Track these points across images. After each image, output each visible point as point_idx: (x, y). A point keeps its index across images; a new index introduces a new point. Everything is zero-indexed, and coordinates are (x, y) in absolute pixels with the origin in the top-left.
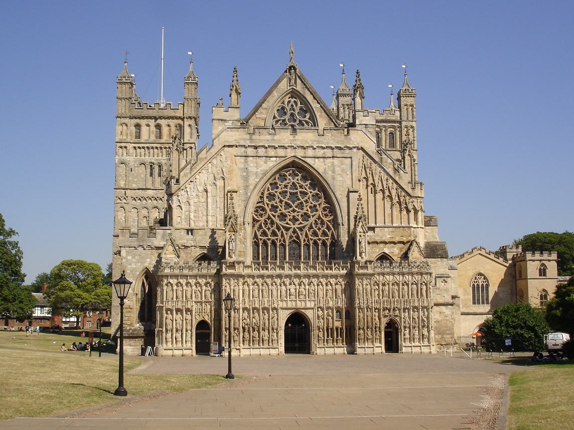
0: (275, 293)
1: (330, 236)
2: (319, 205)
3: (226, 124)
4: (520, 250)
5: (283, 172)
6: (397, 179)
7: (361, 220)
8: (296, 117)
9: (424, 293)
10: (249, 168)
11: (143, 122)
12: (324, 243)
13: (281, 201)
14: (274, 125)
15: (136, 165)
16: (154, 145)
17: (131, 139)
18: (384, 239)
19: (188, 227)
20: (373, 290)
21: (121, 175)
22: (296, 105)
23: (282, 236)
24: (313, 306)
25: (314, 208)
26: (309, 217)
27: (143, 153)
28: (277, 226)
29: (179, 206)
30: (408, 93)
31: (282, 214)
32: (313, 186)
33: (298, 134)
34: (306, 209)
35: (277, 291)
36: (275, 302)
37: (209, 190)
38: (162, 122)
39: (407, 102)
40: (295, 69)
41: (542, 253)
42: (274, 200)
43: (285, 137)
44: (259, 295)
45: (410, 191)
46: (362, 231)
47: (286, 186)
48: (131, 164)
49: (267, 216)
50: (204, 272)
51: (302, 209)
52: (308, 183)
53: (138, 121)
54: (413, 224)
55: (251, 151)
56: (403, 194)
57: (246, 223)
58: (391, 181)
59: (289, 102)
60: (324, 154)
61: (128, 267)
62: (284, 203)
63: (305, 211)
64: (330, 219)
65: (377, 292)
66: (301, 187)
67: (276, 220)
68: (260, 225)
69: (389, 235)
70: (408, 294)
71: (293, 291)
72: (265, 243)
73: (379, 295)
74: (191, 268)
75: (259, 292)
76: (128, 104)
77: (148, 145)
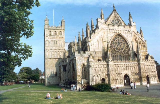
10: (108, 35)
11: (52, 30)
13: (116, 44)
16: (55, 36)
19: (94, 51)
26: (123, 49)
31: (117, 48)
38: (57, 31)
43: (116, 27)
47: (117, 40)
55: (108, 31)
56: (143, 43)
58: (141, 40)
60: (125, 32)
61: (78, 63)
63: (122, 47)
67: (115, 49)
77: (53, 36)
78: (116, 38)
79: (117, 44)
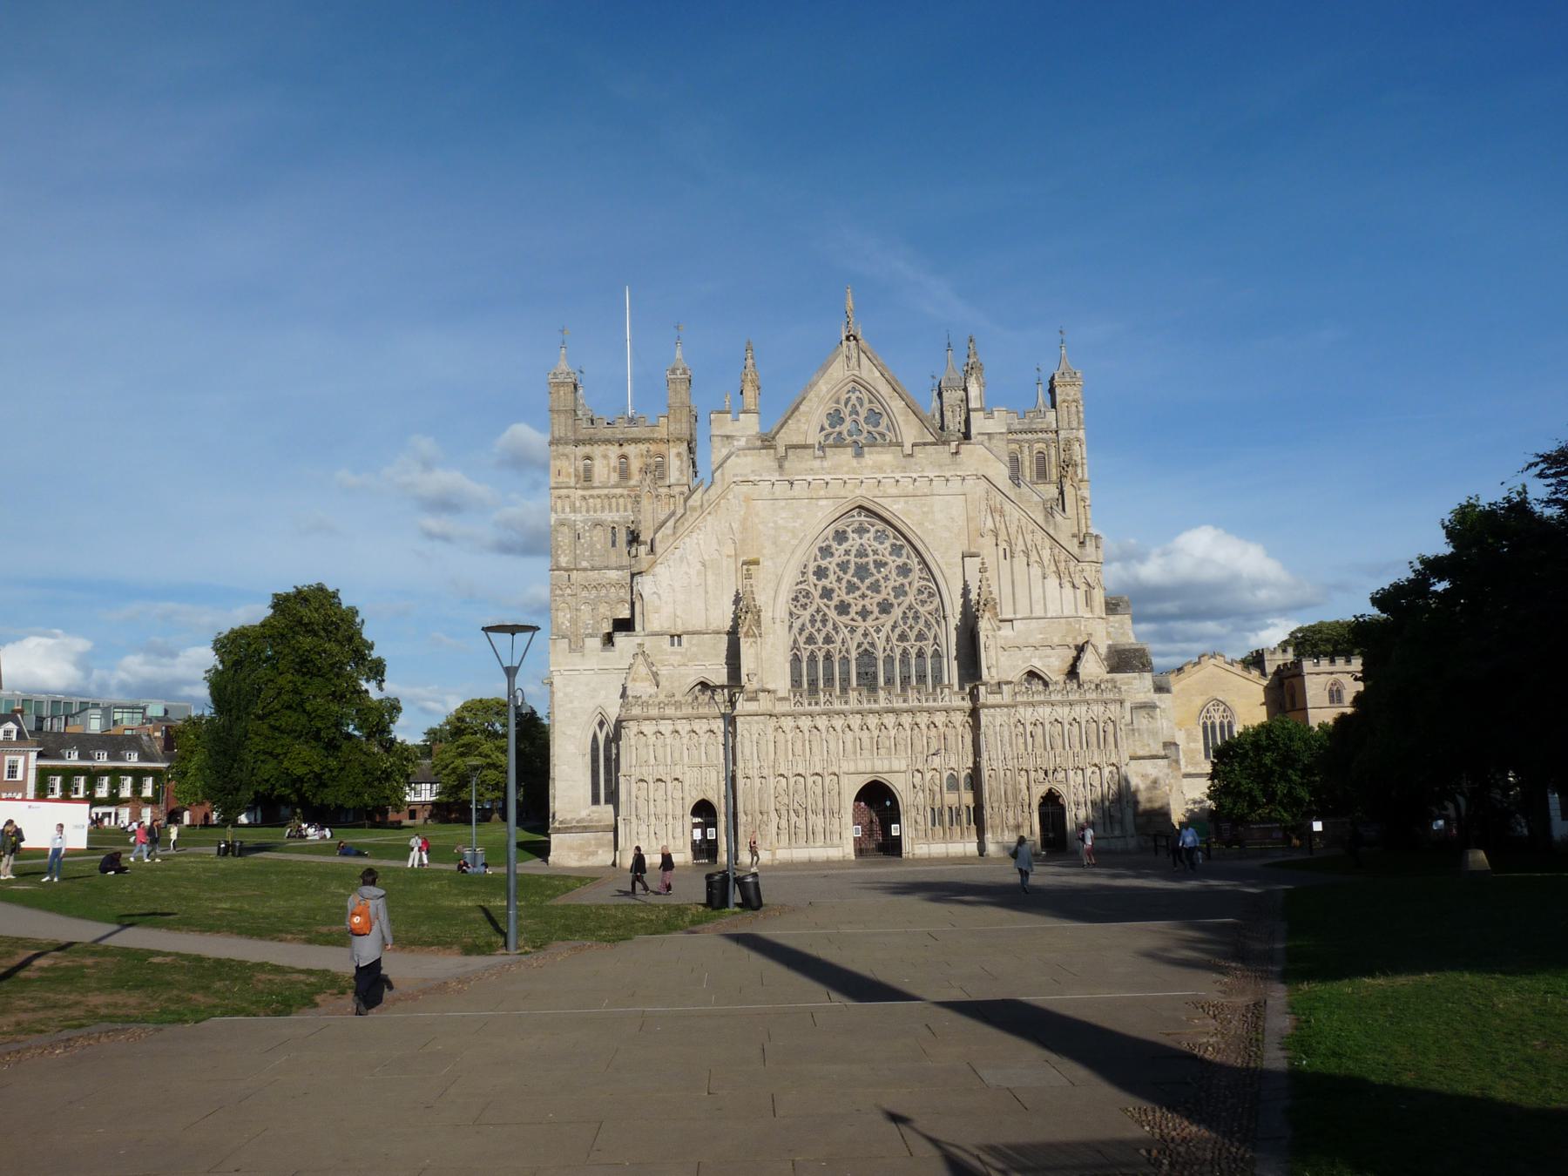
0: (832, 746)
1: (931, 641)
2: (910, 584)
3: (736, 443)
4: (1290, 656)
5: (840, 526)
6: (1052, 532)
7: (986, 609)
8: (863, 427)
9: (1111, 739)
10: (780, 522)
11: (597, 451)
12: (920, 654)
13: (839, 580)
14: (823, 442)
15: (587, 528)
16: (618, 491)
17: (577, 483)
18: (1031, 641)
19: (673, 631)
20: (1014, 737)
21: (561, 547)
22: (861, 405)
23: (843, 642)
24: (904, 768)
25: (900, 591)
26: (892, 605)
27: (599, 506)
28: (834, 625)
29: (655, 593)
30: (1068, 379)
31: (842, 601)
32: (896, 550)
33: (867, 456)
34: (886, 592)
35: (838, 743)
36: (834, 763)
37: (707, 563)
38: (630, 449)
39: (1068, 395)
40: (855, 338)
41: (1332, 661)
42: (826, 577)
44: (804, 751)
45: (1075, 550)
46: (989, 627)
47: (847, 552)
48: (579, 525)
49: (814, 607)
50: (703, 710)
51: (878, 592)
52: (887, 544)
53: (587, 449)
54: (1083, 611)
57: (778, 621)
58: (1040, 534)
59: (848, 400)
62: (844, 582)
63: (883, 595)
64: (931, 607)
65: (1021, 740)
66: (875, 552)
68: (803, 625)
69: (1041, 634)
70: (1081, 742)
71: (866, 742)
72: (812, 658)
73: (1025, 743)
74: (678, 705)
75: (804, 745)
76: (570, 422)
77: (606, 491)
78: (841, 536)
79: (848, 577)
